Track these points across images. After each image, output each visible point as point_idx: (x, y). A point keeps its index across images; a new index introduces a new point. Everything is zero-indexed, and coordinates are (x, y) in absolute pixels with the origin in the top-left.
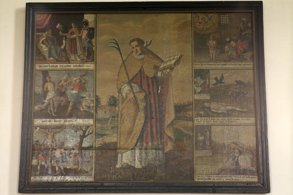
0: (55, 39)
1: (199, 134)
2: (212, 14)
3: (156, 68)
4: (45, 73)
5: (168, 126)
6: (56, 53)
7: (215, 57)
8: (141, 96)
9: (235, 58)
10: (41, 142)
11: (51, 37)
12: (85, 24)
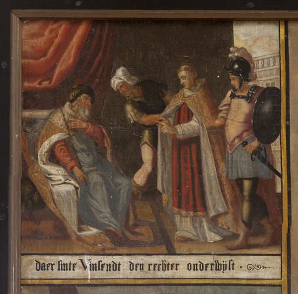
0: (107, 143)
6: (113, 203)
12: (236, 73)
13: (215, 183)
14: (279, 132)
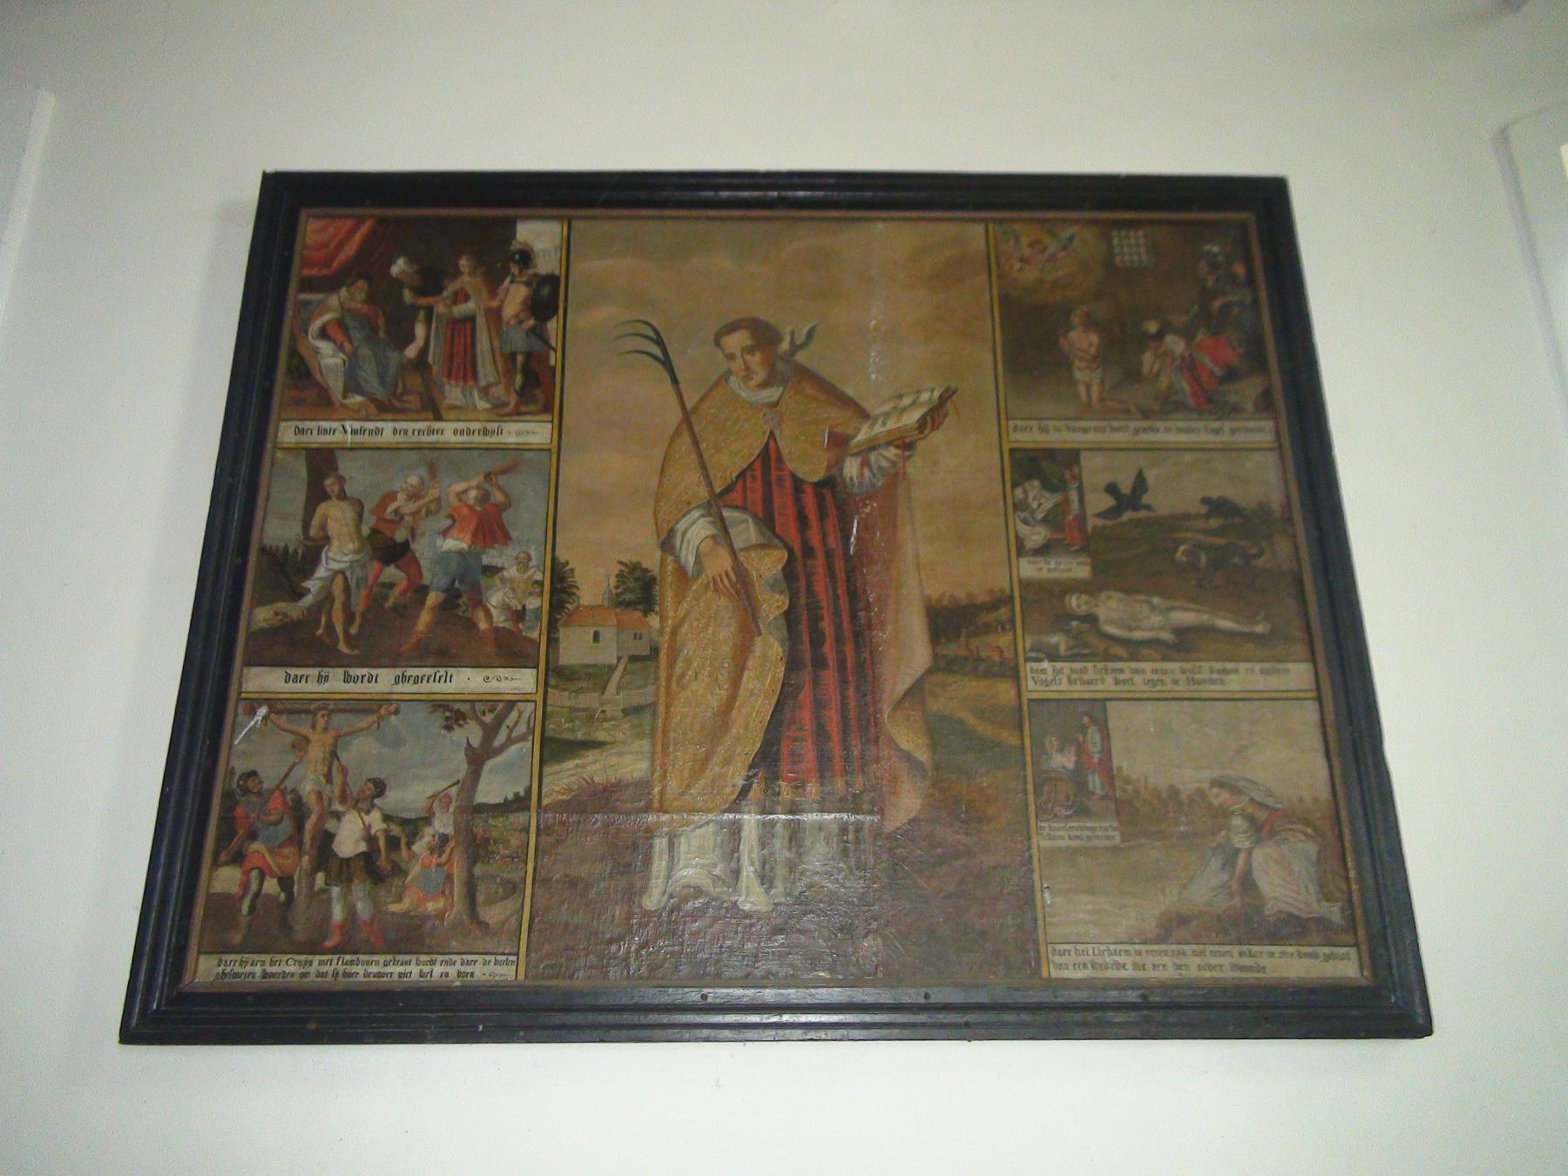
0: (381, 322)
1: (1052, 742)
2: (1074, 229)
3: (839, 442)
4: (322, 462)
5: (898, 705)
6: (382, 376)
7: (1102, 400)
8: (768, 565)
9: (1190, 401)
10: (270, 777)
11: (365, 308)
12: (517, 262)
13: (488, 356)
14: (556, 311)
